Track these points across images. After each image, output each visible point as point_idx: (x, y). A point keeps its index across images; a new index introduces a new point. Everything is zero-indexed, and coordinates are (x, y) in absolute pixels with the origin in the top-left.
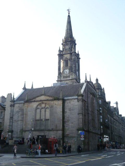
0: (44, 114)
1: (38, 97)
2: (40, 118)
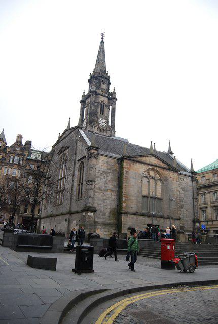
0: (154, 189)
1: (147, 156)
2: (149, 193)
